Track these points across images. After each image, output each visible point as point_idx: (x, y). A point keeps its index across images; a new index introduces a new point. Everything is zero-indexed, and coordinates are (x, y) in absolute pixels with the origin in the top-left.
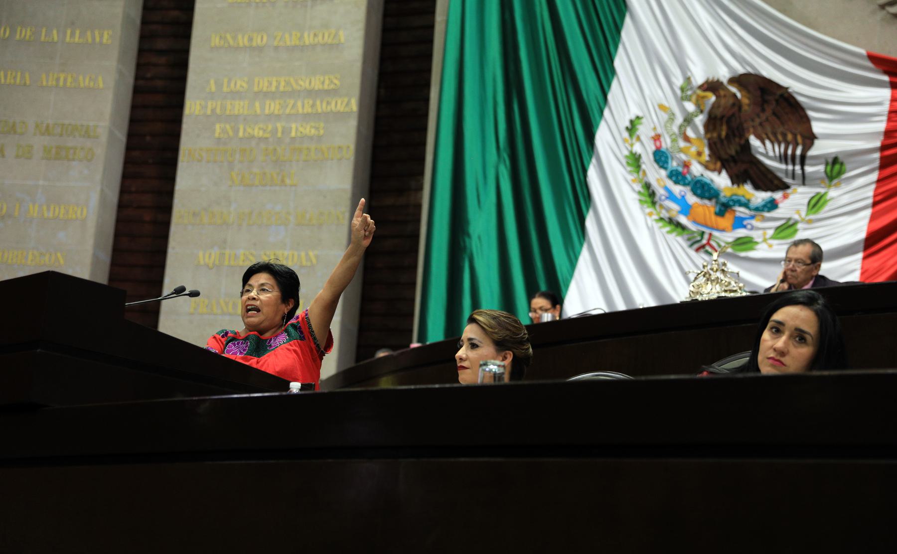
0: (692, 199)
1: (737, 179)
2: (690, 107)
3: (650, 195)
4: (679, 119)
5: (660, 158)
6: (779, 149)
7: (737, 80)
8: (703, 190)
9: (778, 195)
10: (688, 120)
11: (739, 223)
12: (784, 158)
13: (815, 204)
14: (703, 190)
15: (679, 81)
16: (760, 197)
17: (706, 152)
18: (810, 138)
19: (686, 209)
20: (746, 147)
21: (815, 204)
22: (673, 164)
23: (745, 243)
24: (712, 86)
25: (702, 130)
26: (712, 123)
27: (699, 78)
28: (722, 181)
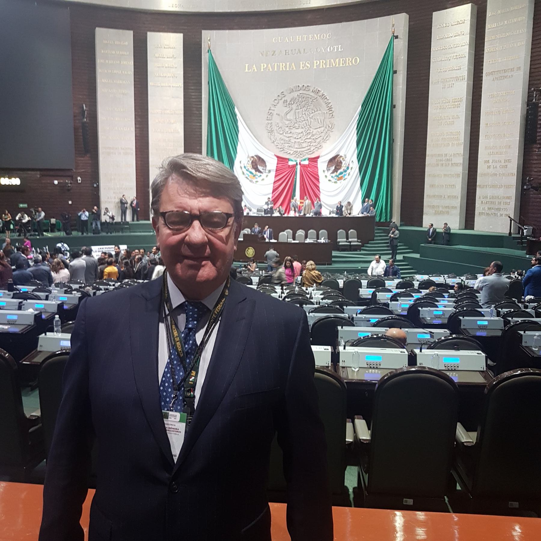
0: (250, 174)
1: (256, 171)
2: (249, 159)
3: (243, 173)
4: (247, 161)
5: (245, 167)
6: (262, 168)
7: (256, 156)
8: (251, 173)
9: (261, 174)
10: (248, 161)
11: (257, 178)
12: (263, 169)
13: (267, 176)
14: (251, 173)
15: (247, 155)
16: (259, 174)
17: (251, 166)
18: (266, 166)
19: (249, 176)
20: (257, 167)
21: (267, 176)
22: (247, 168)
23: (257, 182)
24: (253, 157)
25: (251, 163)
26: (252, 162)
27: (251, 156)
28: (253, 171)
